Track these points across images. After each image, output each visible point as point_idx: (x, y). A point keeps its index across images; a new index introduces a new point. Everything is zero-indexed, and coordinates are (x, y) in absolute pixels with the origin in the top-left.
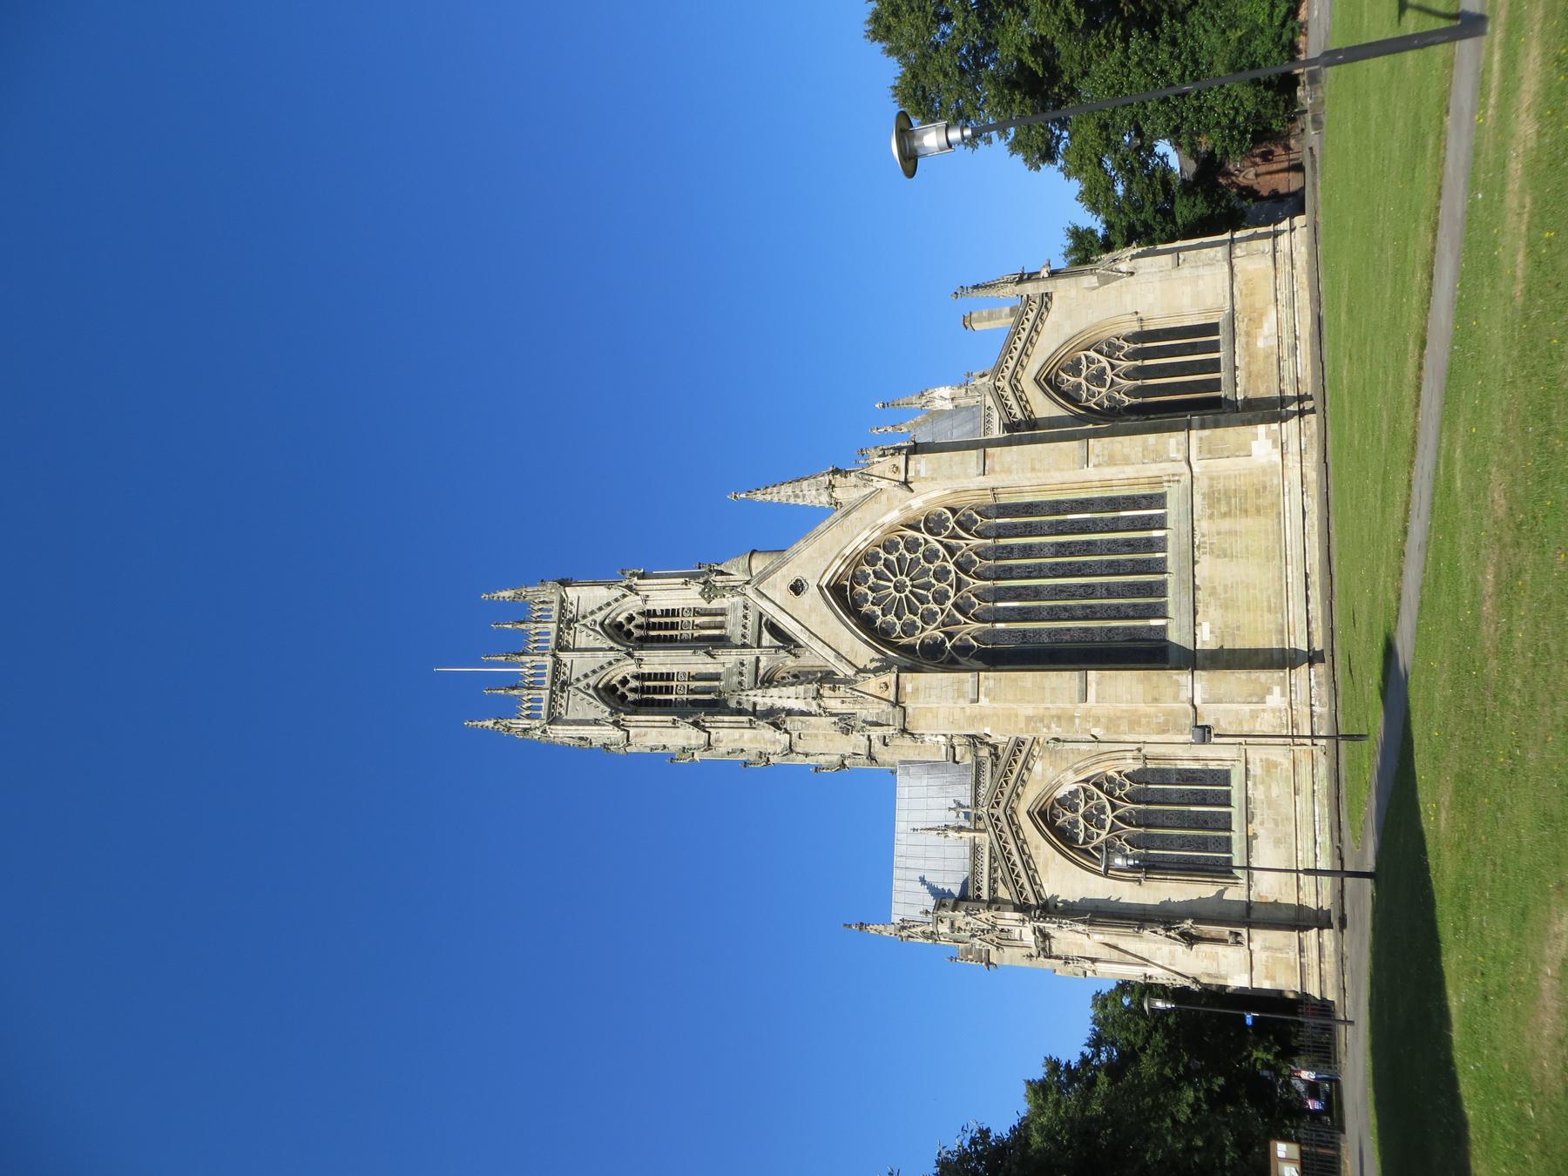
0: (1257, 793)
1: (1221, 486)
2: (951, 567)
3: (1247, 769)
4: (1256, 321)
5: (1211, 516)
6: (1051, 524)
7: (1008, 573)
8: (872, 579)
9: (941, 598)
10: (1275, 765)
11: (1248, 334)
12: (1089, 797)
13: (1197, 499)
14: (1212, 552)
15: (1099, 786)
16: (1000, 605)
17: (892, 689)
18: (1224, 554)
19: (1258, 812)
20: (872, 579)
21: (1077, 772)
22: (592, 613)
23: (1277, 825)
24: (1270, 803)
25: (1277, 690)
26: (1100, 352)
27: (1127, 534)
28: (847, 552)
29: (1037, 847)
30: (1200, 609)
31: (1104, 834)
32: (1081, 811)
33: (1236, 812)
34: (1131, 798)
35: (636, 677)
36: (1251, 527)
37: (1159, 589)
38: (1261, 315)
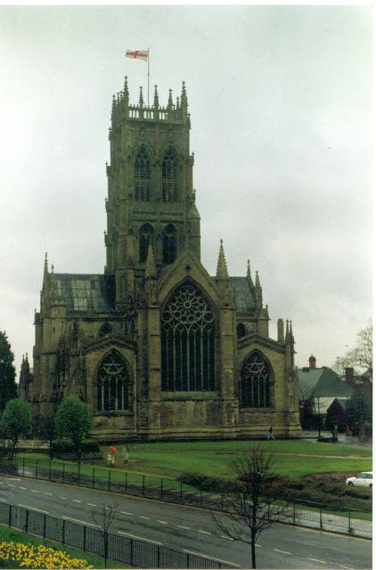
2: (194, 322)
31: (108, 372)
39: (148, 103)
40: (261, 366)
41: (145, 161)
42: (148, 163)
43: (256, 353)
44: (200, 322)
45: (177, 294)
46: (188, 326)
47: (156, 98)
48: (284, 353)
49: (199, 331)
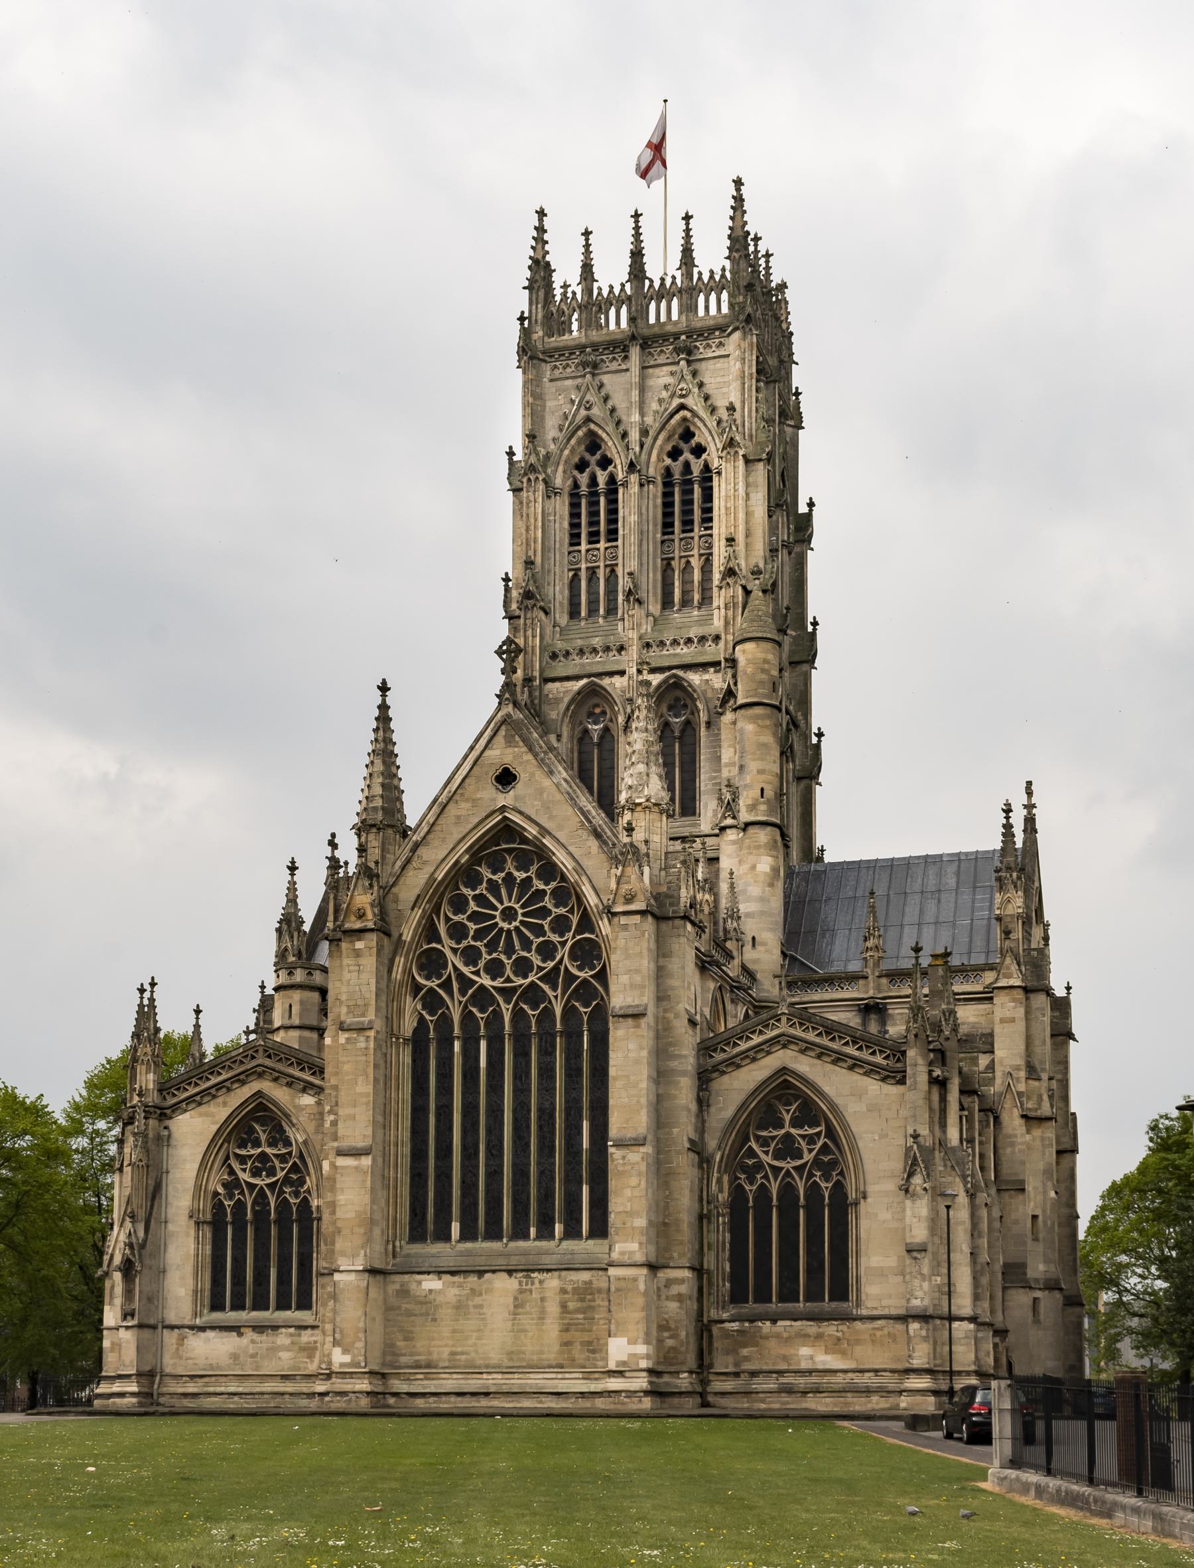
0: (283, 1338)
1: (598, 1302)
3: (306, 1327)
4: (835, 1346)
5: (563, 1291)
6: (578, 1101)
7: (522, 1054)
8: (520, 875)
9: (495, 969)
10: (311, 1357)
11: (819, 1336)
12: (283, 1158)
13: (585, 1276)
14: (521, 1291)
15: (295, 1168)
16: (483, 1045)
17: (358, 925)
18: (518, 1305)
19: (264, 1337)
20: (520, 875)
21: (305, 1142)
23: (253, 1356)
24: (274, 1350)
25: (347, 1359)
26: (825, 1149)
27: (558, 1191)
28: (547, 841)
29: (225, 1104)
30: (456, 1279)
32: (268, 1150)
33: (269, 1316)
34: (283, 1205)
35: (612, 480)
36: (547, 1337)
37: (494, 1233)
38: (843, 1353)
39: (612, 274)
40: (811, 1140)
41: (602, 477)
42: (612, 480)
43: (784, 1089)
44: (551, 977)
45: (473, 880)
46: (507, 993)
47: (637, 255)
48: (902, 1082)
49: (548, 1013)
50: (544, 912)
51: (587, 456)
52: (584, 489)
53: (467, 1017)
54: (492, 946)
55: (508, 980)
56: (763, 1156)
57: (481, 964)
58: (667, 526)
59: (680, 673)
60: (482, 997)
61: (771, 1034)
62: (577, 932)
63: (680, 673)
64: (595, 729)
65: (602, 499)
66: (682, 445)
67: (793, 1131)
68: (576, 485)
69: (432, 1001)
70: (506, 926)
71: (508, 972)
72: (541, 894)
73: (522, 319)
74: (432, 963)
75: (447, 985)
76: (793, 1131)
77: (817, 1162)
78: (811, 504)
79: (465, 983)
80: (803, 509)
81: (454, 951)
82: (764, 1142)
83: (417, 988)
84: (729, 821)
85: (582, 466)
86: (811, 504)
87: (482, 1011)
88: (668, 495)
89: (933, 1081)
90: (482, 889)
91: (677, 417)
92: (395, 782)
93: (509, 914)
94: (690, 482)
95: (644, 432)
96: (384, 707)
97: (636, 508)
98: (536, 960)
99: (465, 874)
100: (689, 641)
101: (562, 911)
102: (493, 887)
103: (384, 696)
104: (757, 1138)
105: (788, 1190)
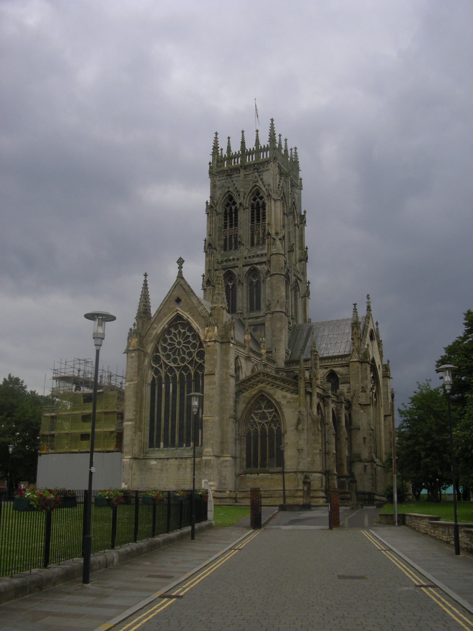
8: (182, 331)
9: (175, 361)
22: (261, 179)
25: (126, 486)
26: (275, 416)
30: (161, 461)
35: (236, 209)
37: (173, 445)
40: (270, 413)
41: (233, 208)
42: (236, 209)
50: (189, 342)
51: (229, 202)
52: (228, 212)
53: (167, 376)
54: (174, 354)
55: (179, 364)
56: (256, 420)
57: (171, 359)
58: (252, 221)
59: (255, 266)
60: (171, 370)
61: (258, 379)
62: (198, 348)
63: (255, 266)
64: (230, 284)
65: (233, 215)
66: (257, 196)
67: (265, 411)
68: (226, 211)
69: (157, 372)
70: (178, 347)
71: (179, 362)
72: (188, 336)
73: (210, 163)
74: (157, 359)
75: (161, 366)
76: (265, 411)
77: (272, 421)
78: (305, 212)
79: (166, 365)
80: (303, 214)
81: (163, 355)
82: (256, 414)
83: (153, 367)
84: (269, 312)
85: (228, 205)
86: (305, 212)
87: (171, 374)
88: (252, 212)
89: (307, 393)
90: (172, 336)
91: (255, 188)
92: (148, 304)
93: (179, 343)
94: (259, 208)
95: (245, 194)
96: (145, 281)
97: (244, 217)
98: (187, 358)
99: (167, 331)
100: (258, 256)
101: (195, 342)
102: (175, 335)
103: (146, 277)
104: (254, 413)
105: (263, 429)
